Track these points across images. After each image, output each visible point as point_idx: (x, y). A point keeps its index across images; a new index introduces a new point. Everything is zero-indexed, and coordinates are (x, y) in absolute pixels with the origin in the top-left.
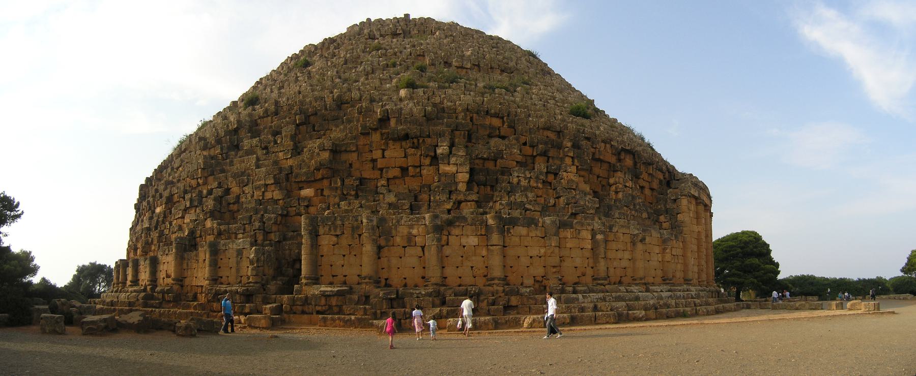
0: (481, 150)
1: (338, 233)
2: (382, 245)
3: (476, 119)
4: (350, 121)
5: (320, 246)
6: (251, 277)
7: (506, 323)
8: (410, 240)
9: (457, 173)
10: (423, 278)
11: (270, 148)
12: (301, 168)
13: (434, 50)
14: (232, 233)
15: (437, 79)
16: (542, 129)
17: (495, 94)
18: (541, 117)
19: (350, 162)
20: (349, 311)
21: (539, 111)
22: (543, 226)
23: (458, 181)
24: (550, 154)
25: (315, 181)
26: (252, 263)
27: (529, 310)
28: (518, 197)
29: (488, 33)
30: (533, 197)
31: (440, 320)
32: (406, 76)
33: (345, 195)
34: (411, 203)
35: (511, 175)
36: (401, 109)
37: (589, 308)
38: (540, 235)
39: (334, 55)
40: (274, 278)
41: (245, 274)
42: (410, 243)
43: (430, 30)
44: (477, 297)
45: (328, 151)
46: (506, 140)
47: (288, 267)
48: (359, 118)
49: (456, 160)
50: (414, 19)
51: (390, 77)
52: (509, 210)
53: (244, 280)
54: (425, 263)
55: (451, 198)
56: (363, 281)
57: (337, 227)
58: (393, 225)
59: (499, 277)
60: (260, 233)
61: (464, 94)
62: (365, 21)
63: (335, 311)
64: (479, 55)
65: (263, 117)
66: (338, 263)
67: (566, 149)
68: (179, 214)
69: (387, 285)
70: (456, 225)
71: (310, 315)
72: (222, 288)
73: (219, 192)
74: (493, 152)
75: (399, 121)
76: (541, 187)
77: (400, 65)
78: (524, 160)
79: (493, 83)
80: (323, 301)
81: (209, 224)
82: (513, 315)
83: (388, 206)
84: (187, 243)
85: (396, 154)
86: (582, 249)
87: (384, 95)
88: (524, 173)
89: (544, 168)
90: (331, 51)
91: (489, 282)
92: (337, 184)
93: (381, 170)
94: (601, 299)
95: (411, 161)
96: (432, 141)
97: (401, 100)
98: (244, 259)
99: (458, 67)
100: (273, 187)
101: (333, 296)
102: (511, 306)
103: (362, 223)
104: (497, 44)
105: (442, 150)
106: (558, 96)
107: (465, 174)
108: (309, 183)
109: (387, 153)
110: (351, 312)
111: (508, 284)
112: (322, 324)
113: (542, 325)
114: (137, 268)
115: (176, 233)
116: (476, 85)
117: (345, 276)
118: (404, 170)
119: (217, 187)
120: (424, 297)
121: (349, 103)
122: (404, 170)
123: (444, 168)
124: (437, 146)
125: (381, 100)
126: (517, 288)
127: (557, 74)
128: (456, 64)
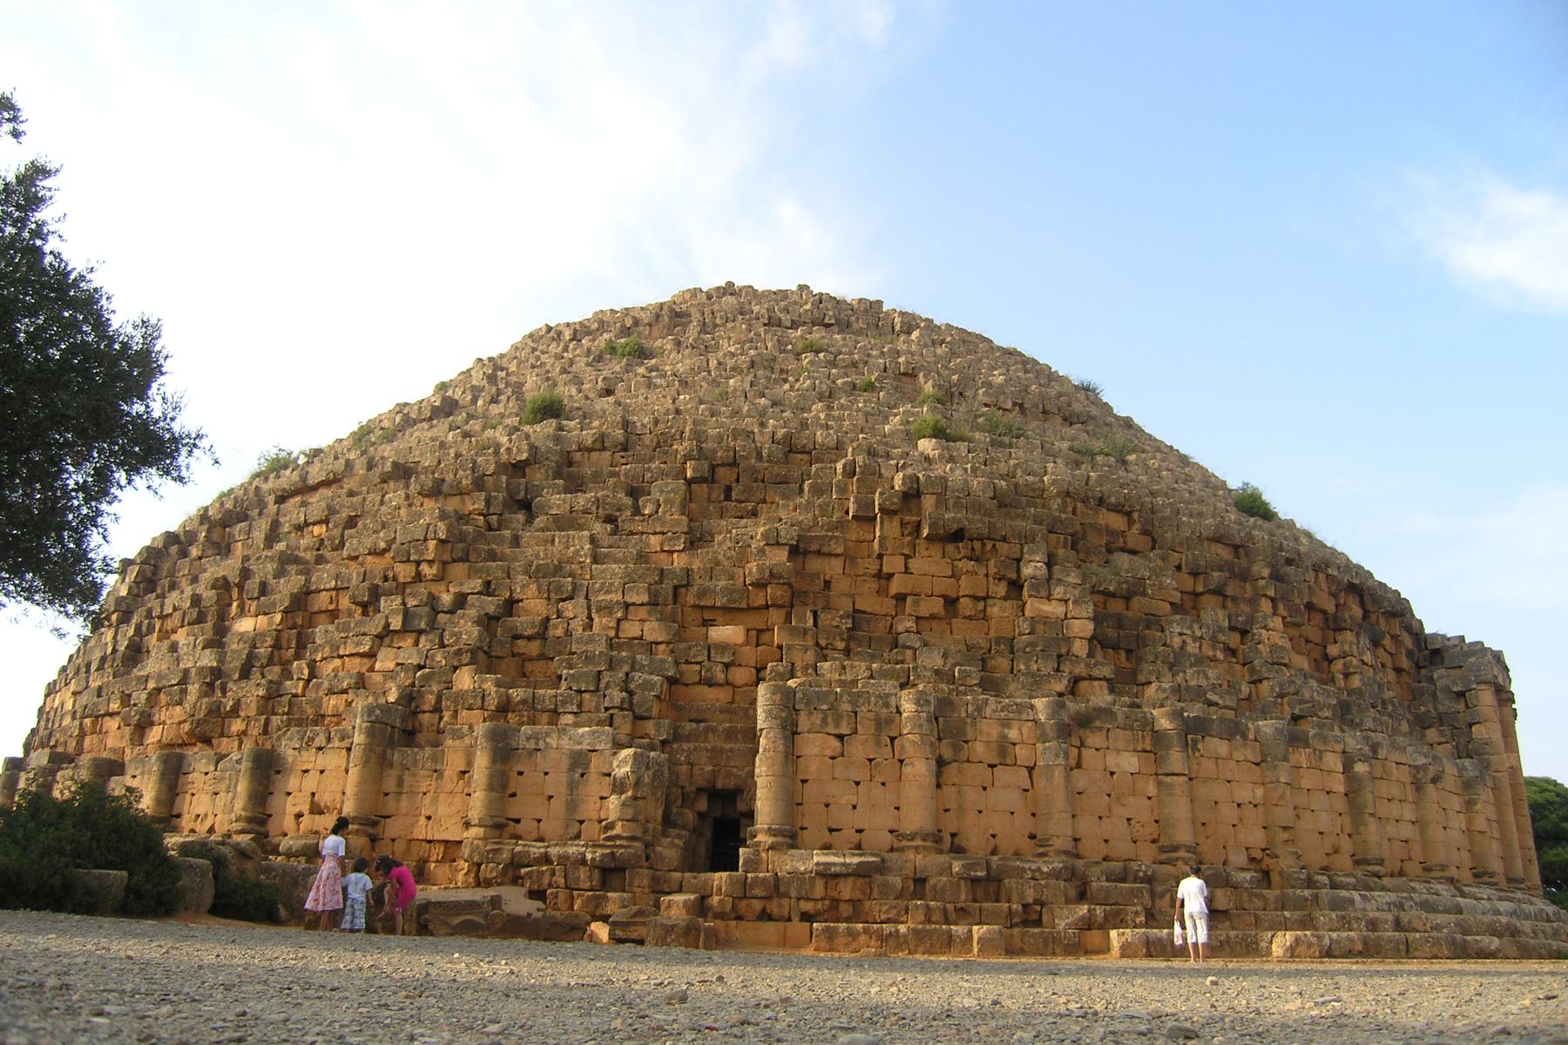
1: (844, 730)
2: (945, 757)
5: (798, 757)
8: (1004, 748)
10: (1032, 837)
16: (1209, 539)
22: (1256, 740)
24: (1230, 591)
25: (750, 609)
28: (1191, 677)
30: (1218, 678)
31: (1089, 932)
33: (822, 649)
38: (1253, 760)
42: (1005, 758)
49: (1065, 593)
56: (905, 843)
59: (1189, 844)
66: (843, 801)
67: (1261, 582)
70: (1096, 728)
74: (1126, 582)
75: (941, 500)
76: (1222, 658)
85: (933, 569)
86: (1328, 793)
88: (1191, 627)
93: (901, 598)
94: (1394, 904)
95: (966, 585)
96: (1010, 548)
103: (899, 712)
105: (1032, 568)
107: (1086, 622)
109: (914, 564)
110: (891, 916)
113: (1315, 951)
117: (859, 831)
118: (951, 602)
120: (1046, 878)
123: (1035, 606)
128: (987, 400)
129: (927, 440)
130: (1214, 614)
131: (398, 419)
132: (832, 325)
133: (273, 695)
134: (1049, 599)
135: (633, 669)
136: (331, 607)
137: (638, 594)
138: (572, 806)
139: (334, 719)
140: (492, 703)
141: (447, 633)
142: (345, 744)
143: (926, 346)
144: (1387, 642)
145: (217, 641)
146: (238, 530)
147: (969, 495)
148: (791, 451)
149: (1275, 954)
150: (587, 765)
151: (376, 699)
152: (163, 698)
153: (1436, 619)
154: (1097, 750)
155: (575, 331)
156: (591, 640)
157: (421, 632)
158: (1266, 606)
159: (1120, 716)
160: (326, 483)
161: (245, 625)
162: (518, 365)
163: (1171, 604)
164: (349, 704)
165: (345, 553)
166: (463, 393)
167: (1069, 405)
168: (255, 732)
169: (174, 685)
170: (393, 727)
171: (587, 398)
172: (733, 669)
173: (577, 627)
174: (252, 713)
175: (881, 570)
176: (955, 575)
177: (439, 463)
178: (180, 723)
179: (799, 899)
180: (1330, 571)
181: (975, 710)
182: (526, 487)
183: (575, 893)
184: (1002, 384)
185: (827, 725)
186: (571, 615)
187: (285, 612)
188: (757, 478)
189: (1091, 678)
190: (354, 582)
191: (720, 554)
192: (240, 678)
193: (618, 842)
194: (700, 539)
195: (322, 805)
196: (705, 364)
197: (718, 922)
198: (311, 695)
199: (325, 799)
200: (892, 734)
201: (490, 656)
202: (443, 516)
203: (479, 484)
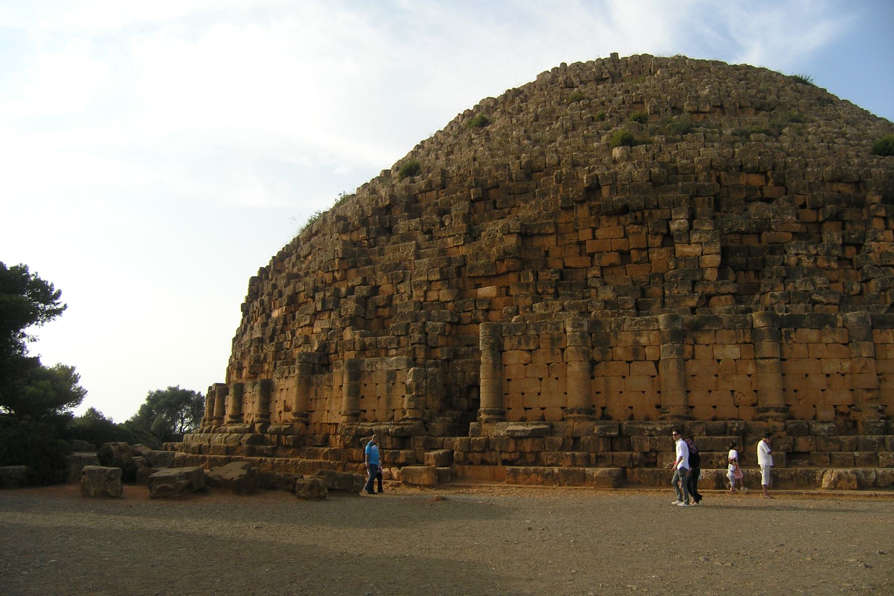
0: (736, 220)
1: (532, 347)
3: (726, 179)
4: (544, 194)
5: (506, 365)
6: (408, 411)
7: (792, 478)
8: (637, 353)
9: (702, 255)
10: (658, 407)
11: (435, 232)
12: (477, 259)
13: (657, 94)
14: (382, 348)
15: (664, 131)
17: (751, 141)
18: (826, 164)
20: (551, 459)
21: (821, 157)
22: (844, 327)
23: (704, 266)
26: (409, 390)
27: (829, 460)
28: (800, 285)
29: (731, 62)
32: (620, 130)
33: (540, 294)
34: (636, 299)
35: (786, 253)
36: (616, 173)
38: (840, 341)
39: (520, 110)
40: (441, 412)
41: (400, 407)
43: (648, 69)
44: (743, 437)
45: (515, 235)
46: (774, 203)
47: (460, 397)
48: (558, 188)
49: (700, 238)
50: (625, 59)
51: (598, 133)
52: (786, 304)
53: (398, 415)
54: (660, 385)
55: (696, 290)
56: (569, 415)
57: (529, 338)
58: (611, 331)
60: (420, 348)
61: (705, 147)
62: (559, 66)
63: (530, 461)
64: (721, 93)
65: (425, 192)
66: (532, 391)
67: (872, 207)
68: (305, 320)
69: (605, 417)
70: (707, 330)
71: (493, 467)
72: (366, 428)
73: (363, 291)
74: (755, 223)
75: (613, 189)
77: (611, 117)
78: (804, 230)
79: (745, 128)
80: (512, 446)
81: (348, 334)
82: (801, 466)
83: (603, 304)
84: (316, 362)
87: (591, 156)
88: (806, 248)
89: (838, 239)
90: (516, 105)
91: (761, 415)
92: (529, 279)
93: (592, 255)
95: (633, 242)
97: (615, 162)
98: (398, 385)
99: (691, 113)
100: (439, 285)
101: (527, 437)
102: (799, 453)
103: (565, 332)
104: (745, 75)
106: (849, 131)
107: (714, 256)
108: (489, 279)
109: (599, 233)
111: (792, 418)
112: (511, 480)
113: (854, 485)
114: (242, 396)
115: (300, 346)
116: (721, 133)
117: (543, 409)
118: (625, 255)
119: (361, 284)
120: (660, 435)
121: (543, 171)
122: (625, 255)
124: (671, 219)
125: (587, 163)
126: (808, 424)
127: (844, 100)
128: (690, 109)
129: (617, 148)
130: (832, 235)
132: (608, 78)
133: (279, 348)
134: (689, 243)
137: (434, 275)
141: (342, 309)
147: (632, 181)
149: (823, 486)
157: (331, 310)
158: (878, 224)
159: (725, 321)
163: (794, 233)
167: (764, 98)
174: (271, 360)
179: (501, 452)
181: (616, 327)
182: (390, 219)
183: (385, 451)
184: (707, 95)
185: (521, 344)
187: (286, 305)
188: (510, 192)
189: (719, 294)
191: (482, 244)
200: (562, 347)
201: (366, 319)
203: (364, 222)
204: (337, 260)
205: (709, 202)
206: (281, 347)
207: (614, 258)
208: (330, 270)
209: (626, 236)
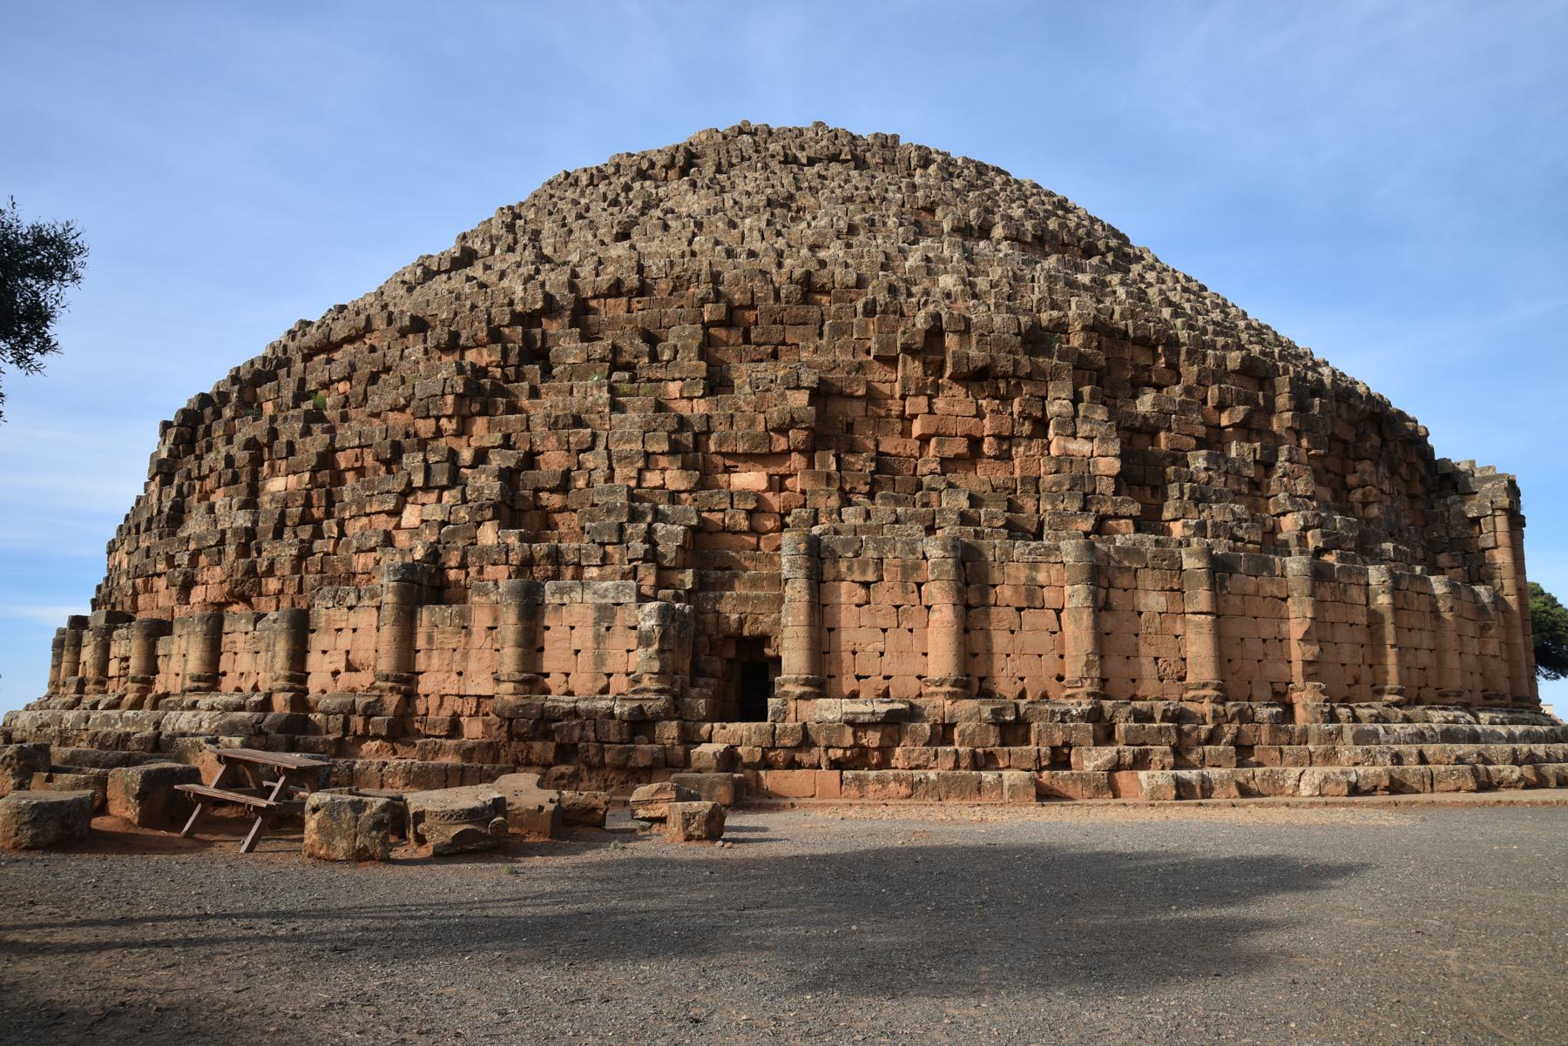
1: (871, 577)
19: (849, 420)
22: (1283, 576)
33: (846, 493)
37: (1410, 754)
49: (1092, 430)
56: (933, 689)
103: (925, 558)
105: (1057, 406)
109: (940, 404)
110: (920, 762)
117: (887, 678)
118: (975, 443)
131: (419, 271)
133: (305, 552)
134: (1074, 435)
135: (655, 520)
136: (357, 465)
138: (599, 660)
139: (365, 576)
140: (515, 558)
142: (374, 603)
143: (943, 179)
144: (1403, 470)
145: (251, 503)
146: (265, 390)
148: (809, 291)
150: (613, 617)
151: (403, 557)
152: (203, 560)
153: (1447, 445)
154: (1125, 590)
155: (592, 175)
156: (612, 492)
157: (442, 489)
160: (350, 340)
161: (277, 485)
162: (536, 213)
163: (1196, 438)
164: (378, 562)
165: (368, 410)
166: (483, 242)
168: (291, 591)
169: (211, 547)
170: (420, 585)
171: (603, 243)
172: (757, 516)
173: (599, 476)
174: (287, 572)
175: (904, 411)
176: (980, 414)
177: (456, 314)
178: (221, 583)
179: (827, 748)
180: (1352, 400)
186: (591, 465)
189: (1117, 517)
190: (378, 439)
192: (274, 538)
193: (647, 695)
194: (720, 385)
195: (358, 661)
196: (720, 205)
197: (748, 771)
198: (342, 552)
199: (358, 657)
200: (919, 580)
202: (460, 370)
203: (495, 335)
204: (452, 397)
205: (1090, 378)
206: (310, 548)
207: (960, 447)
208: (434, 413)
209: (980, 414)
